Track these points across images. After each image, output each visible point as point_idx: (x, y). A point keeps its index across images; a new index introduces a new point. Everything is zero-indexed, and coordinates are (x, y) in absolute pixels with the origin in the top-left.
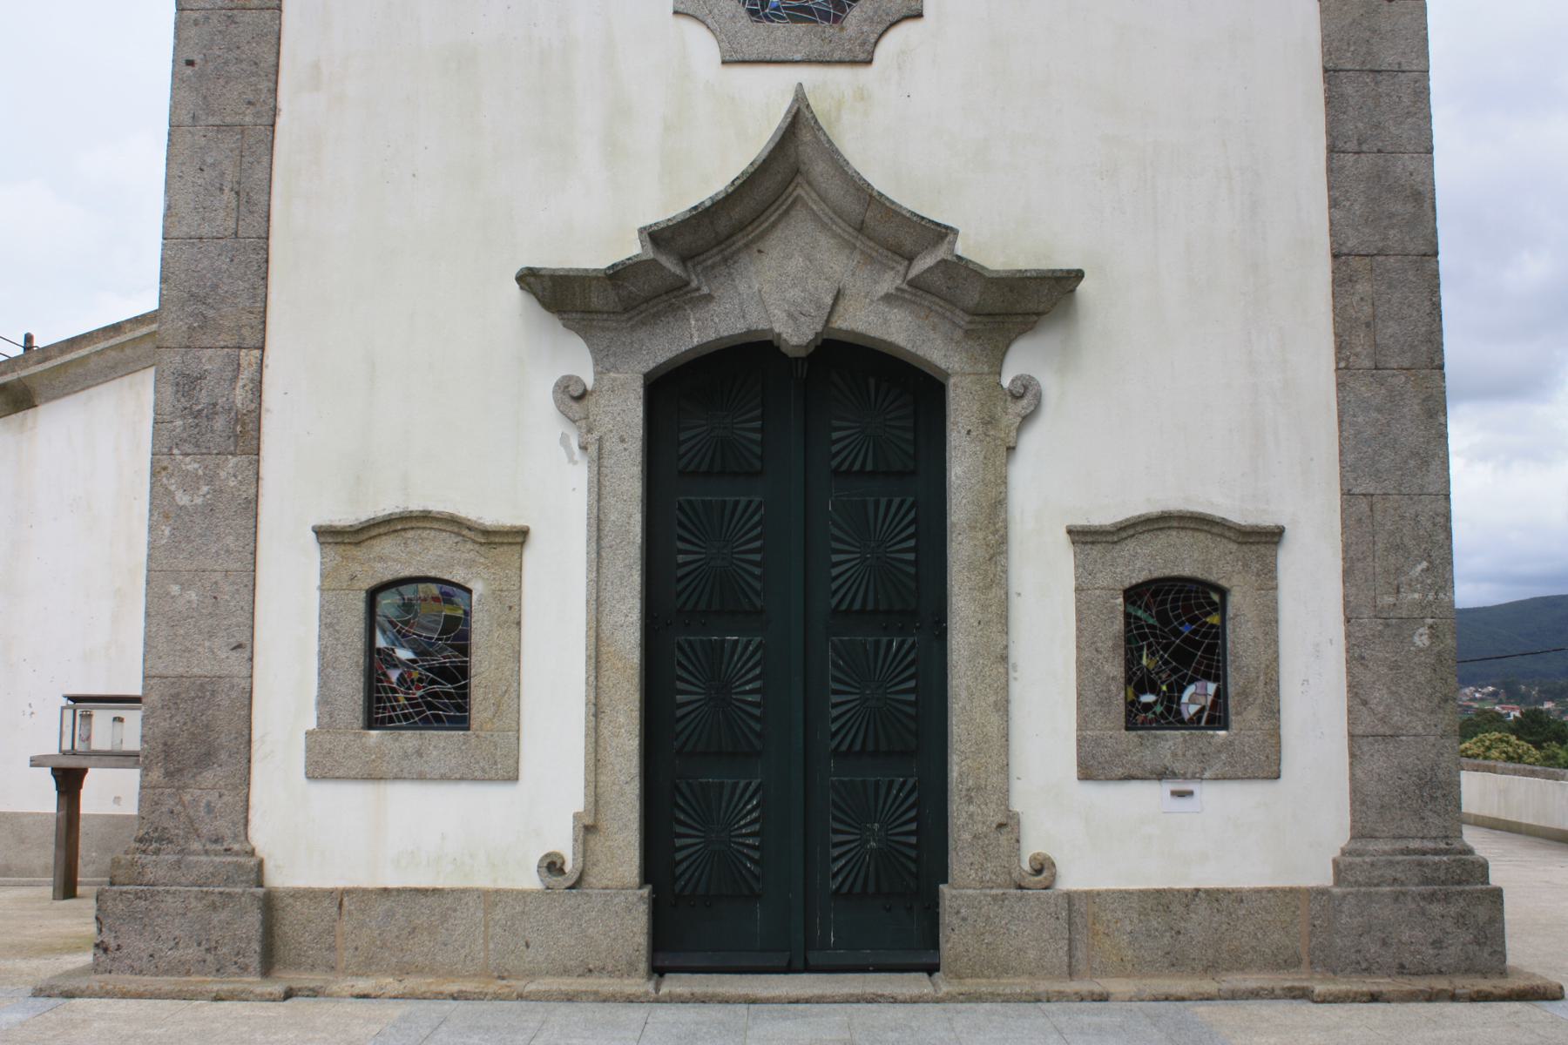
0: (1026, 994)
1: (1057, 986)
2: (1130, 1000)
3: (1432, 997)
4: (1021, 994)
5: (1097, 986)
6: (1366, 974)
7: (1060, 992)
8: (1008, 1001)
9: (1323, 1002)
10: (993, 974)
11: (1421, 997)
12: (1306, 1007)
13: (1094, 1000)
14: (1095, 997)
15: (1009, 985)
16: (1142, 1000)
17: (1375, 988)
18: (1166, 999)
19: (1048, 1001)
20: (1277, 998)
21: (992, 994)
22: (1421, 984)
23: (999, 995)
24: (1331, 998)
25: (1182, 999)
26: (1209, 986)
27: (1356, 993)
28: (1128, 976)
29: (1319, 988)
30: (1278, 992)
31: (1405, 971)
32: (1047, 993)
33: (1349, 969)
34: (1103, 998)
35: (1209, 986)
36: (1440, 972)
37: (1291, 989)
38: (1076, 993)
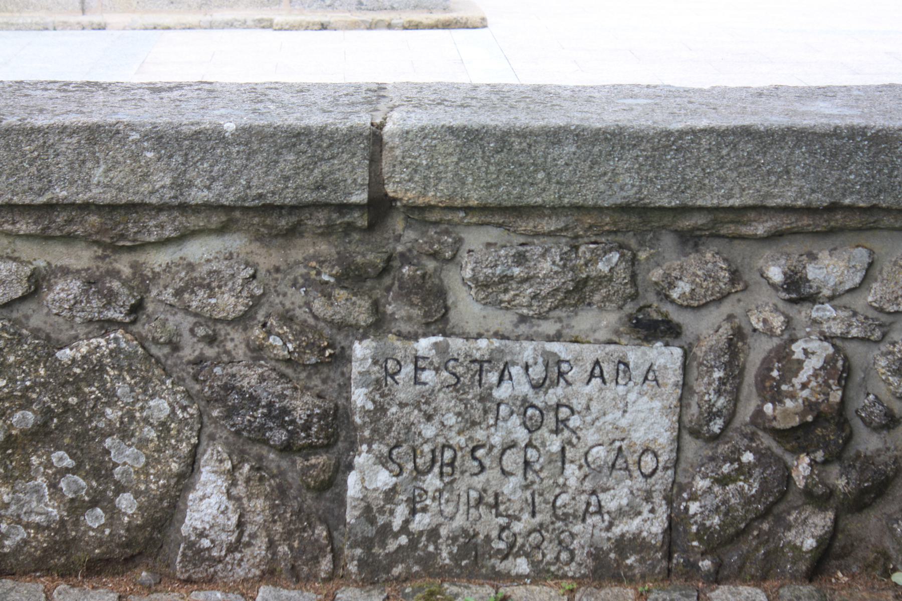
0: (36, 24)
1: (73, 19)
2: (124, 29)
3: (372, 26)
4: (31, 23)
5: (97, 19)
6: (329, 9)
7: (65, 23)
8: (20, 29)
9: (280, 29)
10: (15, 9)
11: (363, 27)
12: (268, 33)
13: (94, 29)
14: (94, 26)
15: (27, 17)
16: (134, 29)
17: (324, 19)
18: (155, 28)
19: (55, 29)
20: (248, 28)
21: (7, 23)
22: (369, 17)
23: (12, 24)
24: (287, 27)
25: (169, 28)
26: (192, 18)
27: (309, 23)
28: (134, 12)
29: (279, 18)
30: (250, 23)
31: (363, 7)
32: (54, 23)
33: (315, 5)
34: (102, 27)
35: (192, 18)
36: (393, 8)
37: (260, 21)
38: (78, 23)
